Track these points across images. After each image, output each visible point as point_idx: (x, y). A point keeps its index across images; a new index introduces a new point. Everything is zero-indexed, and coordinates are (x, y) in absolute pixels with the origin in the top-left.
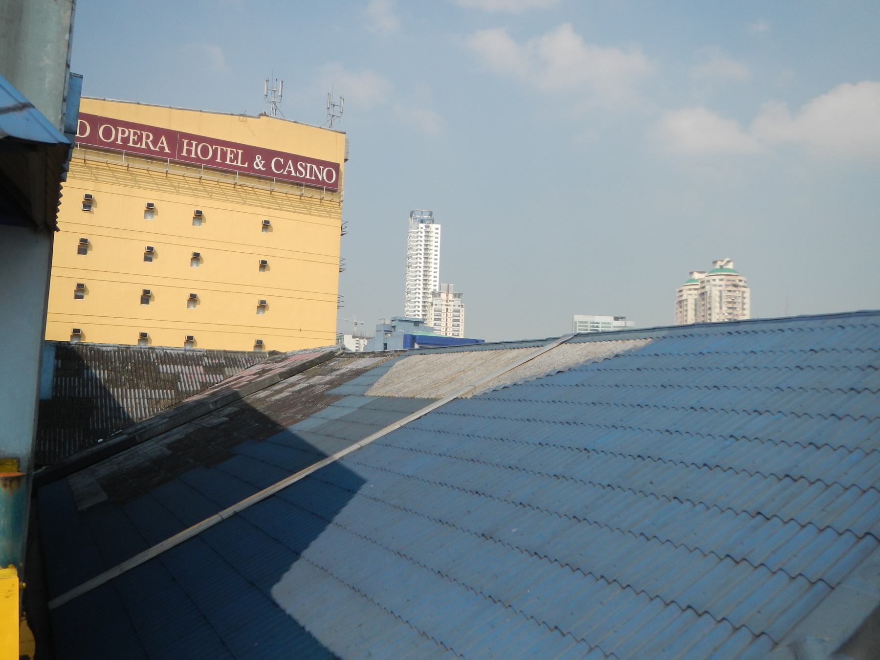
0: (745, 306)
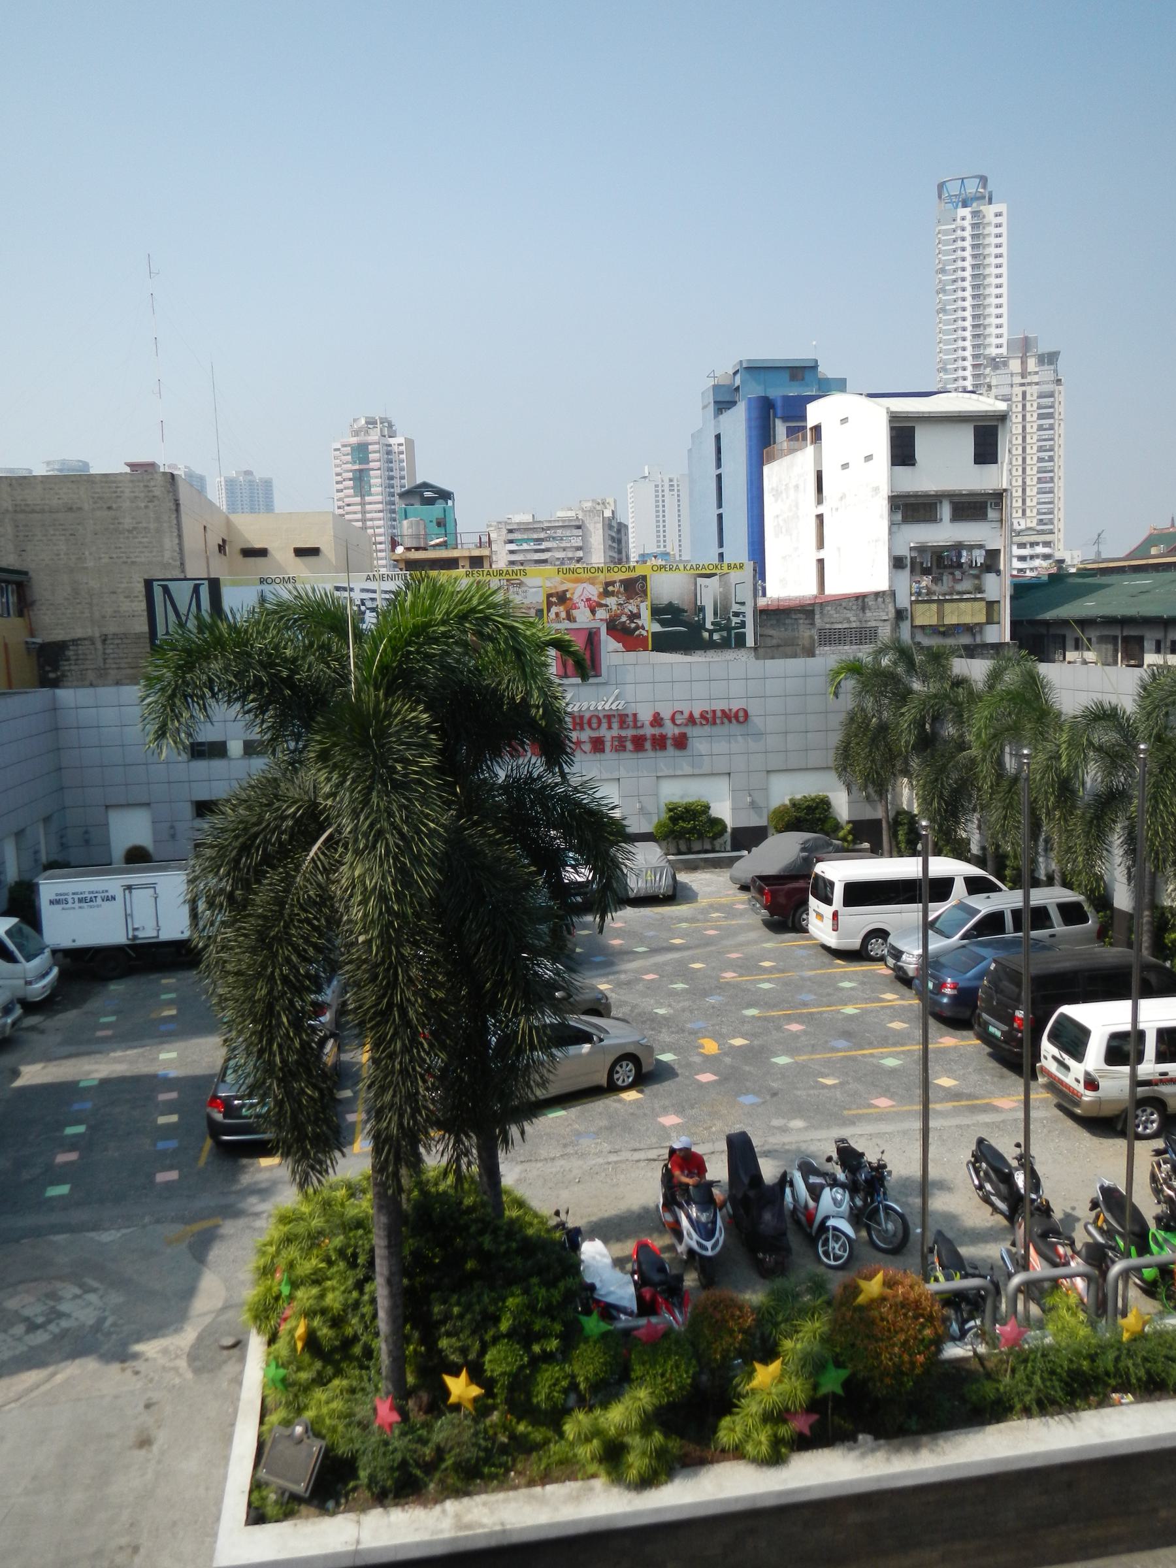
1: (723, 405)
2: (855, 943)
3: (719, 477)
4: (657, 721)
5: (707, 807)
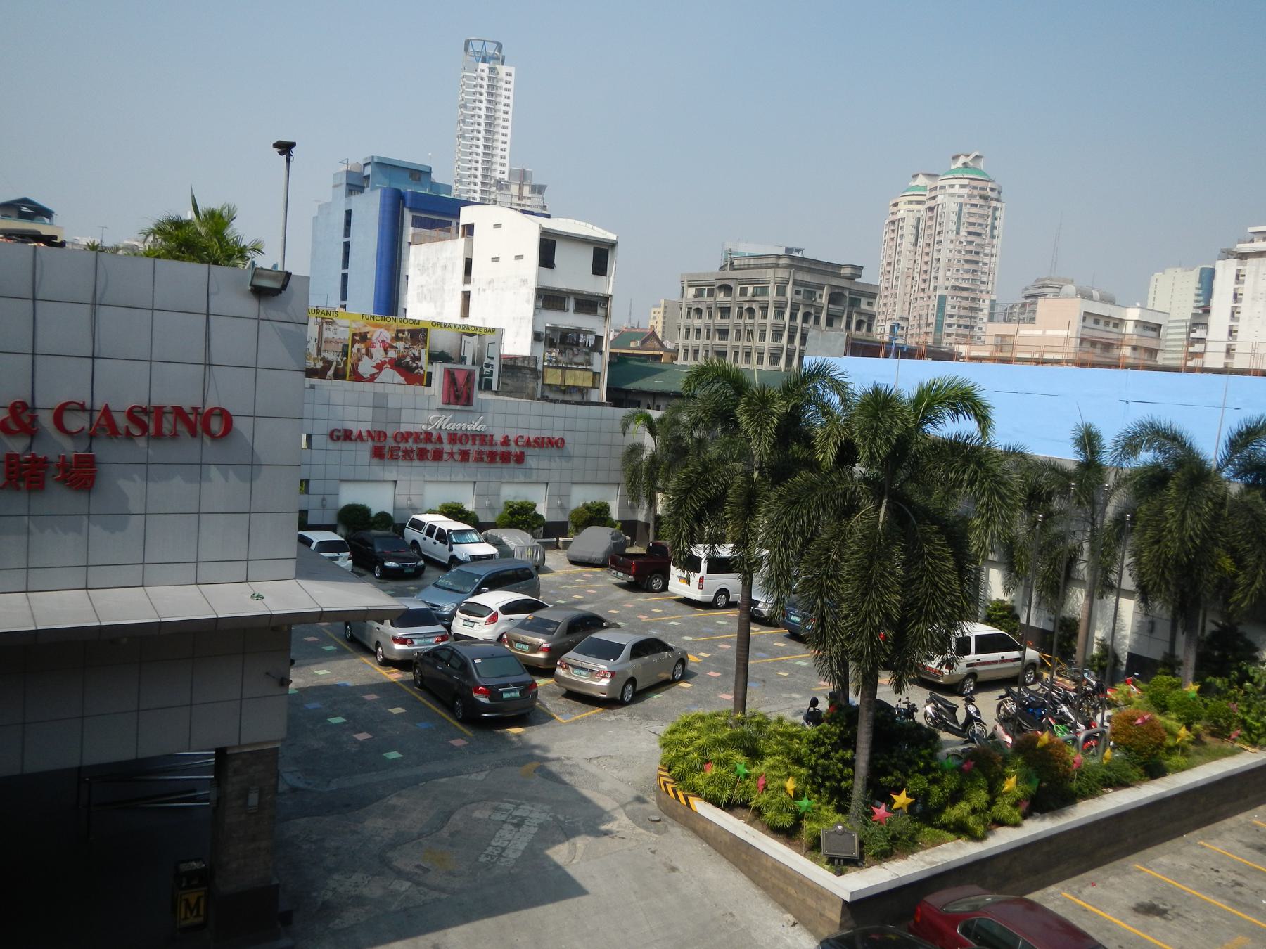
0: (996, 232)
1: (355, 185)
2: (710, 597)
3: (347, 245)
4: (506, 441)
5: (534, 506)
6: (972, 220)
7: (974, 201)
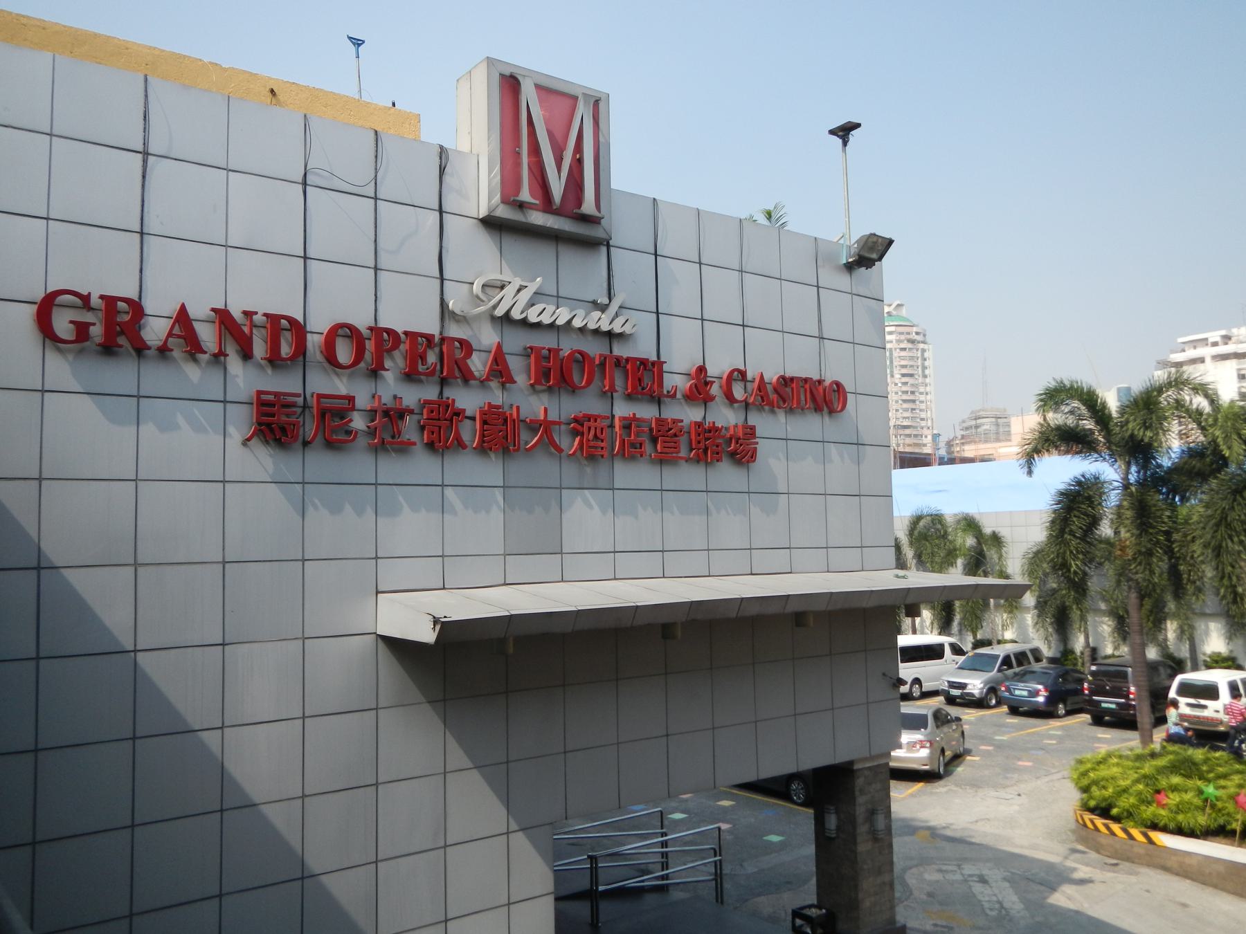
0: (927, 372)
6: (903, 363)
7: (902, 346)
